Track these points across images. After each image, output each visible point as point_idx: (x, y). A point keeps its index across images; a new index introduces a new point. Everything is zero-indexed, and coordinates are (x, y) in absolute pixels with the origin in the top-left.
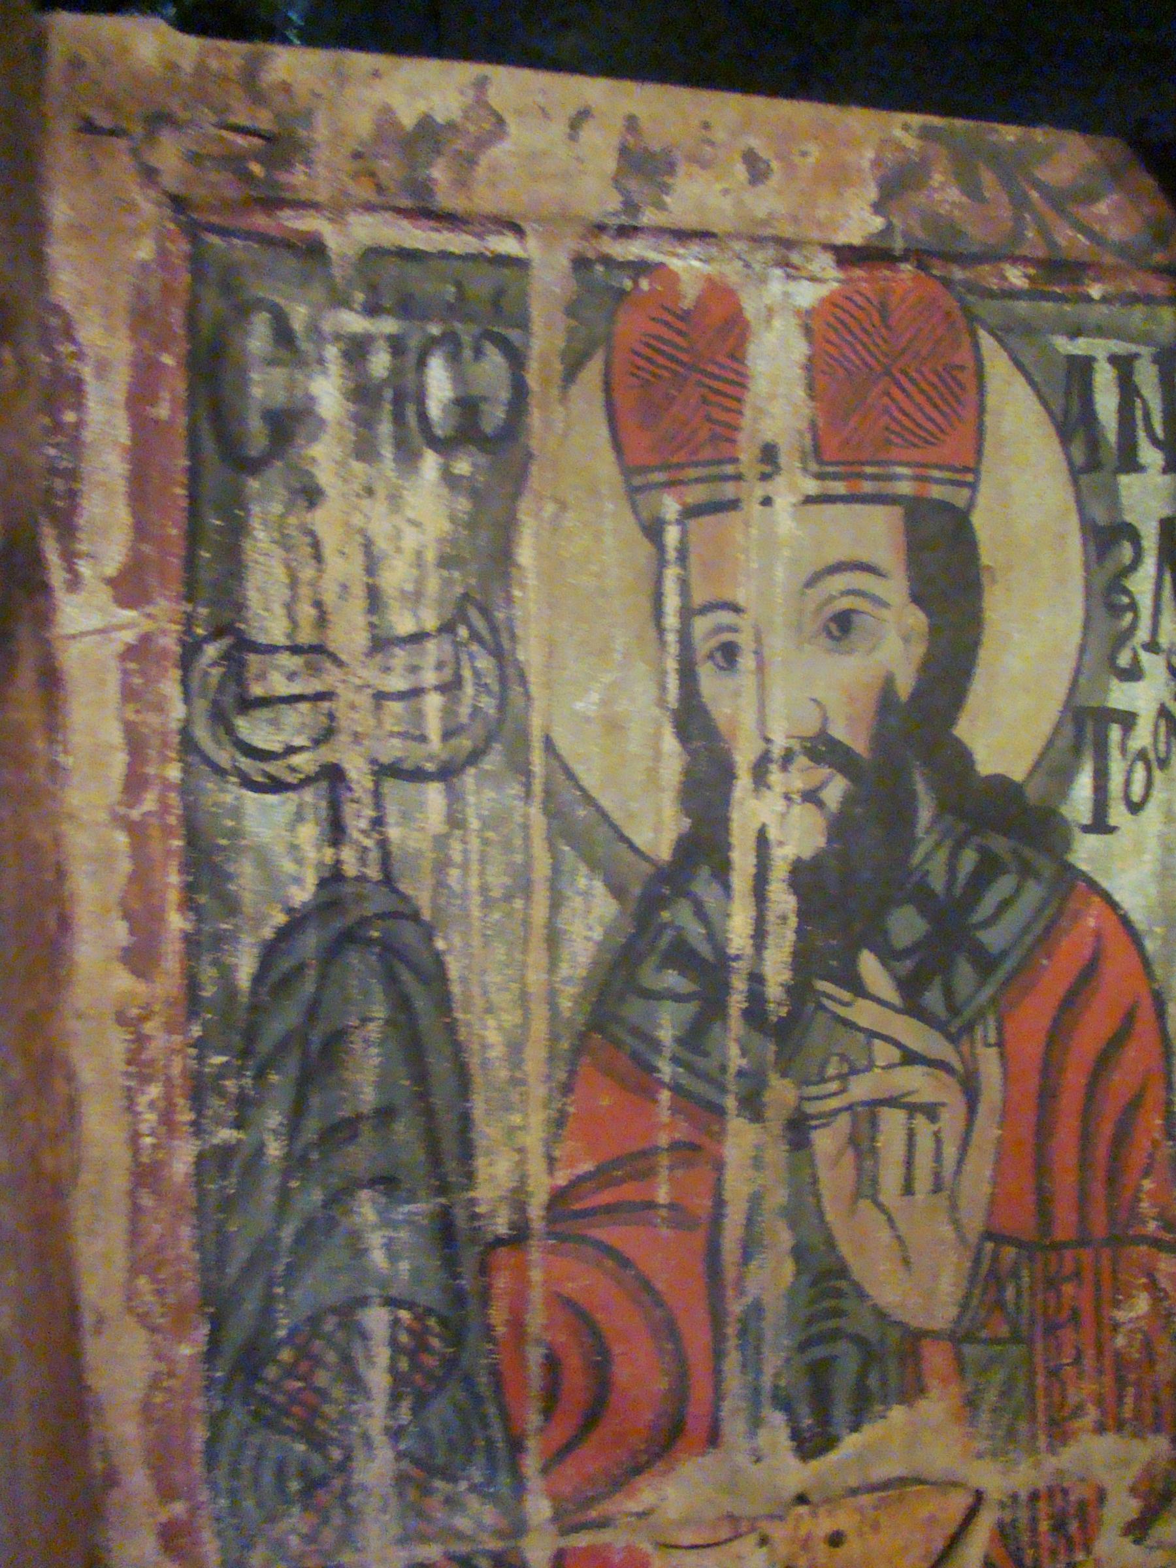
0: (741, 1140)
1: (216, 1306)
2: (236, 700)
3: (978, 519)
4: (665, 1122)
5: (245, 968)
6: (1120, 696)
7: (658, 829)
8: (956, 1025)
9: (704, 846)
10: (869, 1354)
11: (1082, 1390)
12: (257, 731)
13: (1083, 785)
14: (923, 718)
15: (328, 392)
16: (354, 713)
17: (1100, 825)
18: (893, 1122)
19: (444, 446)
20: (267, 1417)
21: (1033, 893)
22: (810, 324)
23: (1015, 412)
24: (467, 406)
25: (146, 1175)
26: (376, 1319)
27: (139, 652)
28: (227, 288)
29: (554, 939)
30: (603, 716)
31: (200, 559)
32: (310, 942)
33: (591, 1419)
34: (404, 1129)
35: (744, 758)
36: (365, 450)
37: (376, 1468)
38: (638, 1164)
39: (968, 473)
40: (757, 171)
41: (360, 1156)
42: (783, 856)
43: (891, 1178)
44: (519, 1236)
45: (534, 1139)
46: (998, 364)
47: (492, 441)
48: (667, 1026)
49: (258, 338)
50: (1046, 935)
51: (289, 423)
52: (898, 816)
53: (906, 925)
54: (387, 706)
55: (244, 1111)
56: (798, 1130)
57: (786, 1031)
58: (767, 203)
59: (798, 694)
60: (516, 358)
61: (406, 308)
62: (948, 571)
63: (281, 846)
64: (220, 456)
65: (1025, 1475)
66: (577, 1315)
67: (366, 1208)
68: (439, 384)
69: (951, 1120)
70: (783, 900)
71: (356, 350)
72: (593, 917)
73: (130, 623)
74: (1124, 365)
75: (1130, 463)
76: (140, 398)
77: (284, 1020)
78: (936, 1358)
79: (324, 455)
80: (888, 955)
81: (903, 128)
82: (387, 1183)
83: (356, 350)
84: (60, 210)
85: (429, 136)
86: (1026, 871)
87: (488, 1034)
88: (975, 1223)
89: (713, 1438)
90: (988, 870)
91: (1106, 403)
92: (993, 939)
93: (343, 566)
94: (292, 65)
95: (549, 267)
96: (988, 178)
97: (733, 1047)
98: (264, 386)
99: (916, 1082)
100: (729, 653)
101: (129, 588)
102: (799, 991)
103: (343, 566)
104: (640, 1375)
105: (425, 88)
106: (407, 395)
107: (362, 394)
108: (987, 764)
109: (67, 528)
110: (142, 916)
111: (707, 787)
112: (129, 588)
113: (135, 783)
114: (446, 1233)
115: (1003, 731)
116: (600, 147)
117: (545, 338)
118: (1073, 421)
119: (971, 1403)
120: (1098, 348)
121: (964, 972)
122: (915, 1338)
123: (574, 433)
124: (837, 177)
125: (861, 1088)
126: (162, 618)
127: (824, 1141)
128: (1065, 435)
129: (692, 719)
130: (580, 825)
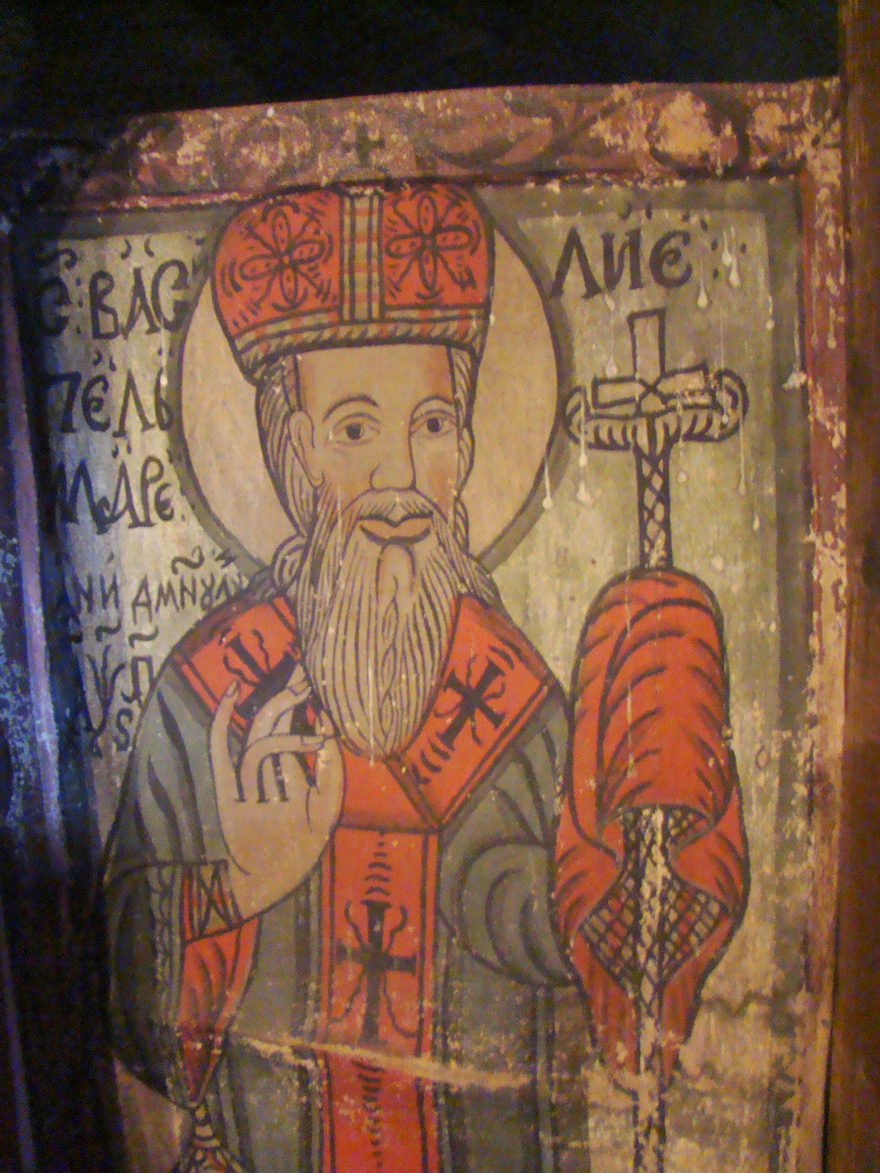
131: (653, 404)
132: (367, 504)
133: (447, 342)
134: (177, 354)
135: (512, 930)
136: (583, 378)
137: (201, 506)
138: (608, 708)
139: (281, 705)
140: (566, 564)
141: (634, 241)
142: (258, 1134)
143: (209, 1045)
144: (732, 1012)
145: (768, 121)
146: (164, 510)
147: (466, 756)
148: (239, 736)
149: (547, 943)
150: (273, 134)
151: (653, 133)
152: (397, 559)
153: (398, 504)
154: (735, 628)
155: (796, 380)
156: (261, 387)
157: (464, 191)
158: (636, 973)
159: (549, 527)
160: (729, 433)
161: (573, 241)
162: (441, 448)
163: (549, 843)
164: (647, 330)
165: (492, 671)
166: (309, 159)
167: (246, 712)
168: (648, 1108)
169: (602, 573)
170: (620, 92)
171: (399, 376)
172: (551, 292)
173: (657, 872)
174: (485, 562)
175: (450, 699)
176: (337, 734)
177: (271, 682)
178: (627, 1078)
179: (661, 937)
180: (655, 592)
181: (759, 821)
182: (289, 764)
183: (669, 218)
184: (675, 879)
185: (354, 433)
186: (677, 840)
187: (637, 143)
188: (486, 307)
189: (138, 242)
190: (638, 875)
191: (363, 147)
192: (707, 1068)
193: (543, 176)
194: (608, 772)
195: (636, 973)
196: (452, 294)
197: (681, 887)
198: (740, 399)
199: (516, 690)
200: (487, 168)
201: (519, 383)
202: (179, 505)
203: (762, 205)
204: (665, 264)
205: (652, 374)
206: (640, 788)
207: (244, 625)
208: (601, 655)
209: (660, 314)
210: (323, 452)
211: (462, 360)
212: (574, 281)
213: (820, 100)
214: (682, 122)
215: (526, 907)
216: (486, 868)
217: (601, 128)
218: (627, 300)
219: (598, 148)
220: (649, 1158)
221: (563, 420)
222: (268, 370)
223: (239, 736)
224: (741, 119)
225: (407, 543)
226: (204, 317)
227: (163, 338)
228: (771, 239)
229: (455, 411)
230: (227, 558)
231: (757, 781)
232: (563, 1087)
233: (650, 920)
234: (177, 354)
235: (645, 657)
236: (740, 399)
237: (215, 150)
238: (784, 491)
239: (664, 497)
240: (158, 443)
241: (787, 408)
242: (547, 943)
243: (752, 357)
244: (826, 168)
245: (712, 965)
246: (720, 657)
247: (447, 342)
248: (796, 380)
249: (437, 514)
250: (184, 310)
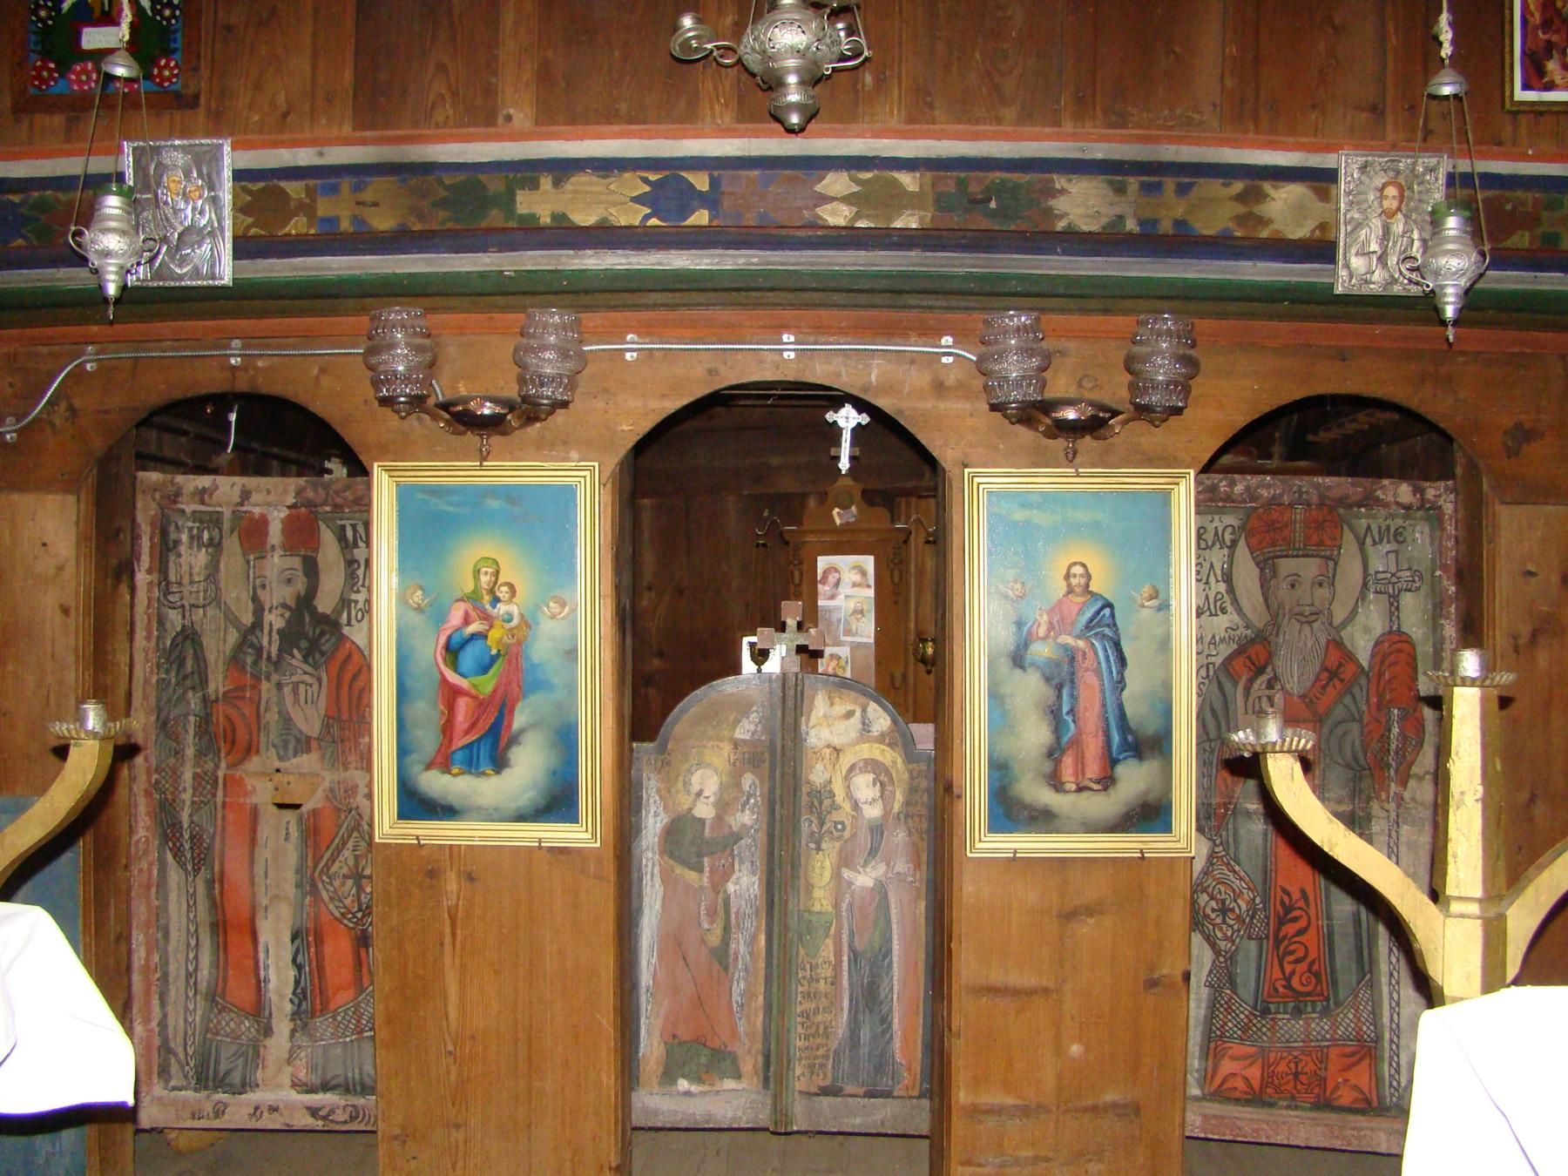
0: (265, 686)
1: (159, 710)
2: (167, 593)
3: (319, 559)
4: (248, 680)
5: (168, 643)
6: (354, 596)
7: (247, 619)
8: (316, 667)
9: (258, 624)
10: (298, 741)
11: (352, 758)
12: (171, 598)
13: (345, 615)
14: (306, 601)
15: (185, 537)
16: (186, 593)
17: (349, 624)
18: (302, 687)
19: (207, 547)
20: (168, 736)
21: (333, 640)
22: (282, 521)
23: (327, 536)
24: (211, 539)
25: (147, 681)
26: (192, 719)
27: (151, 583)
28: (168, 518)
29: (225, 640)
30: (236, 596)
31: (161, 567)
32: (180, 639)
33: (233, 743)
34: (196, 676)
35: (267, 607)
36: (191, 548)
37: (190, 752)
38: (242, 688)
39: (316, 550)
40: (269, 492)
41: (188, 682)
42: (275, 628)
43: (302, 699)
44: (217, 700)
45: (220, 679)
46: (323, 526)
47: (216, 546)
48: (249, 660)
49: (172, 528)
50: (336, 649)
51: (177, 543)
52: (301, 620)
53: (304, 644)
54: (192, 592)
55: (167, 672)
56: (279, 686)
57: (277, 664)
58: (271, 498)
59: (279, 594)
60: (221, 530)
61: (201, 521)
62: (311, 569)
63: (175, 619)
64: (165, 548)
65: (336, 777)
66: (228, 719)
67: (190, 694)
68: (206, 535)
69: (315, 687)
70: (275, 637)
71: (191, 529)
72: (233, 637)
73: (149, 578)
74: (354, 527)
75: (356, 545)
76: (151, 539)
77: (177, 652)
78: (314, 744)
79: (183, 549)
80: (299, 650)
81: (302, 481)
82: (193, 688)
83: (191, 529)
84: (139, 505)
85: (204, 490)
86: (332, 634)
87: (211, 657)
88: (322, 712)
89: (258, 751)
90: (323, 633)
91: (350, 534)
92: (324, 648)
93: (185, 568)
94: (180, 479)
95: (227, 513)
96: (320, 490)
97: (264, 665)
98: (173, 536)
99: (307, 678)
100: (264, 586)
101: (149, 572)
102: (280, 656)
103: (185, 568)
104: (242, 734)
105: (205, 481)
106: (200, 537)
107: (191, 537)
108: (320, 610)
109: (139, 560)
110: (149, 632)
111: (259, 611)
112: (149, 572)
113: (148, 607)
114: (205, 699)
115: (324, 604)
116: (237, 490)
117: (226, 526)
118: (341, 537)
119: (323, 757)
120: (347, 523)
121: (318, 655)
122: (309, 739)
123: (232, 544)
124: (285, 492)
125: (295, 679)
126: (155, 577)
127: (287, 690)
128: (340, 541)
129: (255, 599)
130: (231, 619)
131: (1394, 580)
132: (1296, 610)
133: (1327, 558)
134: (1231, 557)
135: (1348, 752)
136: (1371, 571)
137: (1239, 610)
138: (1380, 675)
139: (1265, 677)
140: (1367, 630)
141: (1388, 528)
142: (1243, 847)
143: (1227, 810)
144: (1420, 779)
145: (1430, 493)
146: (1223, 611)
147: (1331, 692)
148: (1247, 690)
149: (1360, 756)
150: (1269, 486)
151: (1395, 495)
152: (1306, 628)
153: (1307, 610)
154: (1419, 650)
155: (1438, 573)
156: (1262, 570)
158: (1389, 766)
159: (1361, 618)
160: (1418, 589)
161: (1369, 528)
162: (1324, 592)
163: (1361, 721)
164: (1392, 556)
165: (1341, 665)
166: (1281, 495)
167: (1251, 682)
168: (1393, 815)
169: (1378, 631)
170: (1386, 482)
171: (1309, 568)
172: (1362, 544)
173: (1396, 730)
174: (1338, 629)
175: (1326, 674)
176: (1282, 688)
177: (1260, 671)
178: (1386, 805)
179: (1397, 753)
180: (1396, 638)
182: (1264, 700)
183: (1399, 522)
184: (1401, 733)
185: (1293, 586)
186: (1403, 719)
187: (1390, 499)
188: (1340, 548)
189: (1217, 517)
190: (1389, 730)
191: (1300, 493)
192: (1413, 799)
193: (1360, 506)
194: (1380, 696)
195: (1389, 766)
196: (1328, 542)
197: (1403, 736)
198: (1421, 578)
199: (1348, 672)
200: (1342, 501)
202: (1230, 609)
203: (1428, 519)
204: (1399, 537)
205: (1393, 570)
206: (1391, 701)
207: (1252, 651)
208: (1378, 658)
209: (1396, 552)
210: (1282, 591)
211: (1331, 564)
212: (1369, 541)
213: (1446, 488)
214: (1405, 492)
215: (1353, 745)
216: (1339, 730)
217: (1379, 493)
219: (1378, 499)
220: (1394, 835)
221: (1365, 585)
222: (1267, 567)
223: (1247, 690)
224: (1422, 491)
225: (1310, 623)
226: (1242, 543)
227: (1226, 551)
228: (1432, 529)
229: (1328, 580)
230: (1247, 627)
232: (1363, 810)
233: (1393, 747)
234: (1231, 557)
235: (1392, 658)
236: (1421, 578)
237: (1248, 488)
238: (1435, 607)
239: (1398, 608)
240: (1222, 587)
241: (1435, 582)
242: (1360, 756)
243: (1424, 565)
244: (1448, 508)
245: (1413, 763)
246: (1414, 659)
247: (1327, 558)
248: (1438, 573)
250: (1234, 543)
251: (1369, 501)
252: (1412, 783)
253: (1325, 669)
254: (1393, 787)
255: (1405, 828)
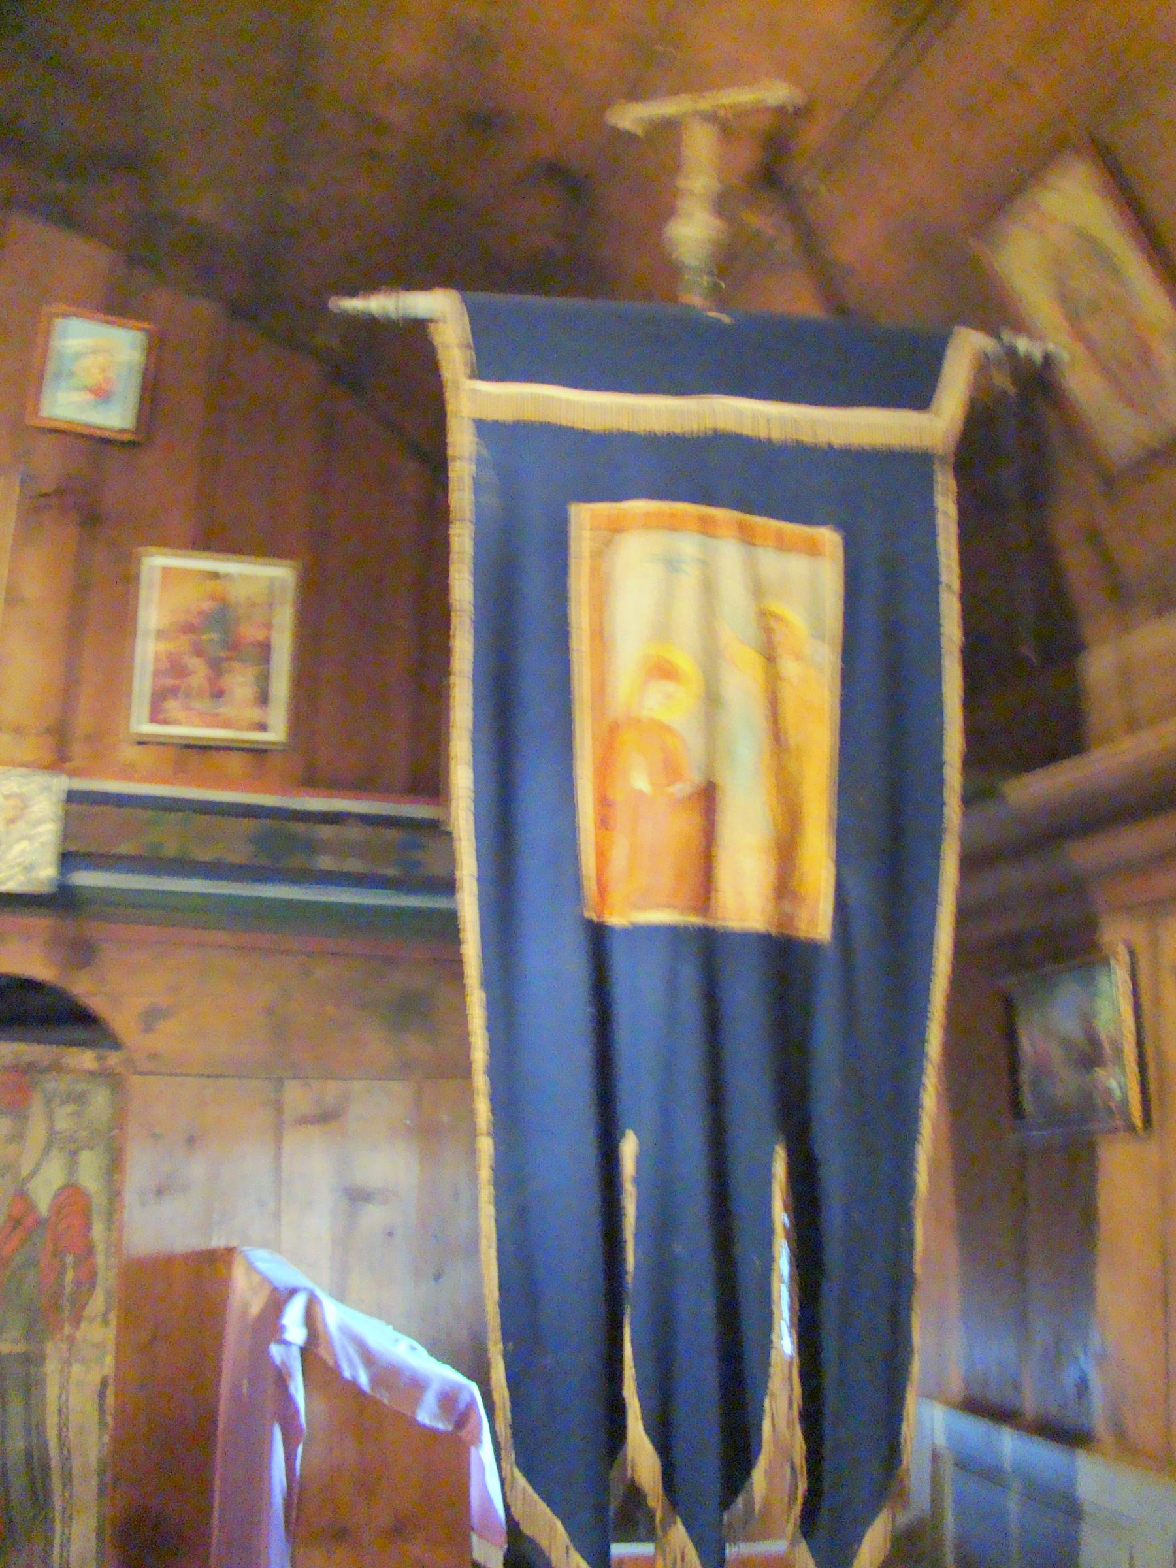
144: (92, 1320)
157: (26, 1072)
173: (70, 1275)
181: (100, 1259)
186: (76, 1266)
192: (84, 1340)
197: (78, 1284)
201: (37, 1132)
204: (80, 1099)
218: (70, 1108)
229: (18, 1137)
231: (100, 1247)
249: (10, 1168)
251: (56, 1067)
252: (84, 1324)
253: (10, 1217)
254: (67, 1330)
255: (76, 1369)
